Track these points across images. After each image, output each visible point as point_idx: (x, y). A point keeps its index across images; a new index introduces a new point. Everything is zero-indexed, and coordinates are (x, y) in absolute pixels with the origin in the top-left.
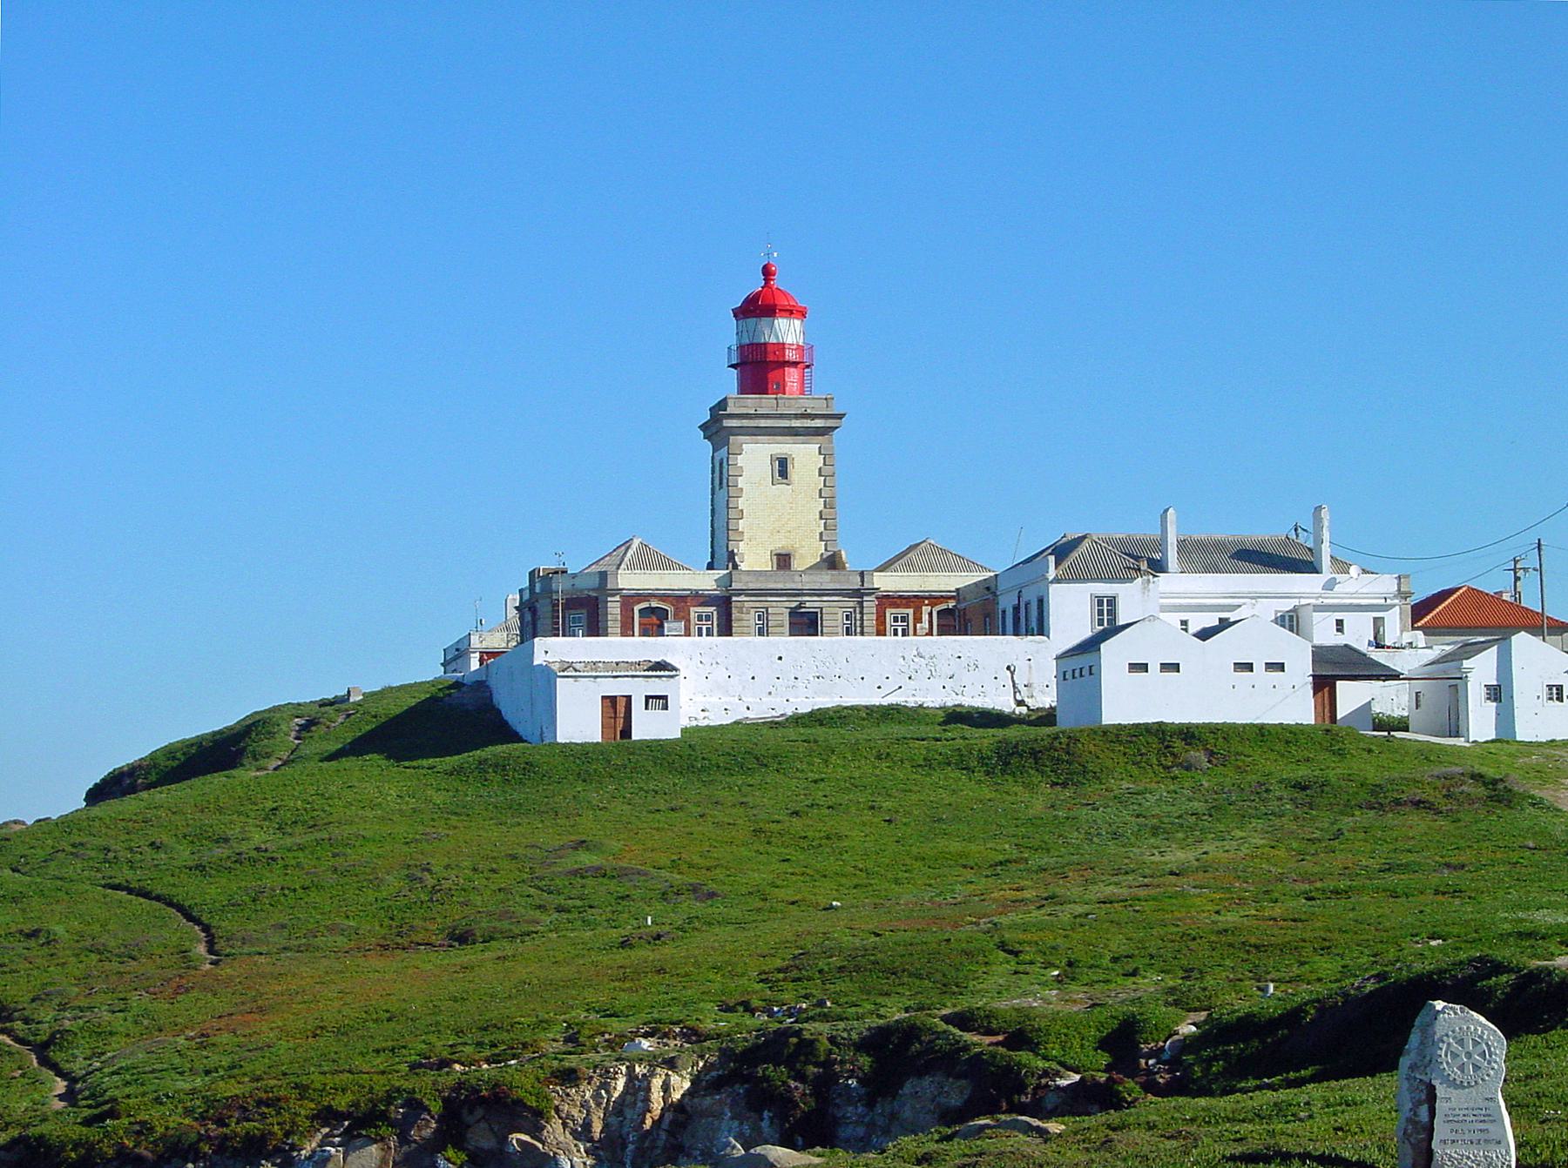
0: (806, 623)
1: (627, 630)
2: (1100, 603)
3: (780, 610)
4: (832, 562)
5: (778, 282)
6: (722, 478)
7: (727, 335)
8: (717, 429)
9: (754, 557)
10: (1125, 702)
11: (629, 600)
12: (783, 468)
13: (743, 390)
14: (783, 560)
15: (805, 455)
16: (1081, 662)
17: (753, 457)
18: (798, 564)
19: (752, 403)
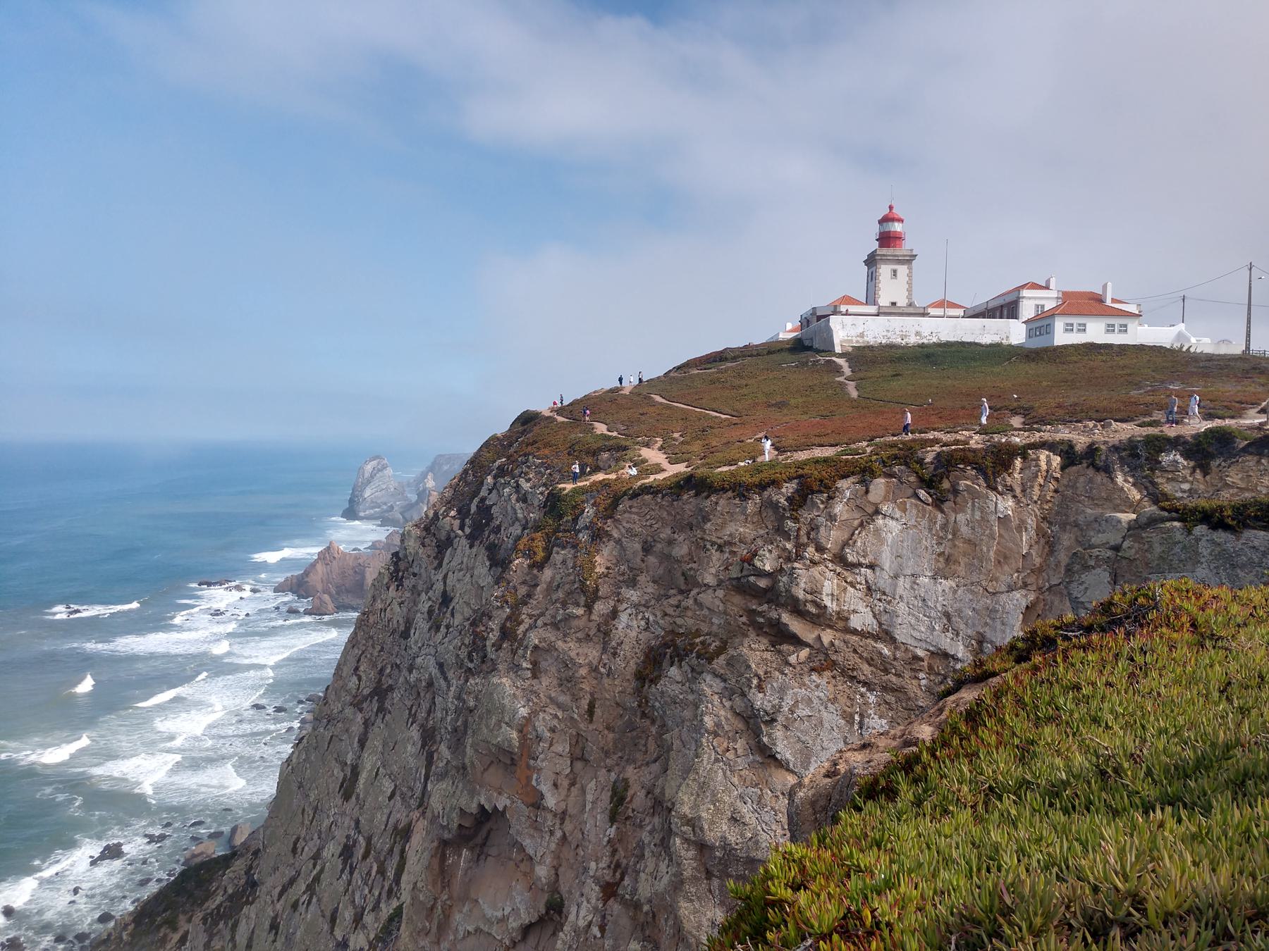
2: (1037, 306)
4: (910, 305)
6: (872, 278)
7: (875, 230)
10: (1062, 336)
13: (881, 246)
15: (902, 270)
17: (884, 270)
19: (884, 251)
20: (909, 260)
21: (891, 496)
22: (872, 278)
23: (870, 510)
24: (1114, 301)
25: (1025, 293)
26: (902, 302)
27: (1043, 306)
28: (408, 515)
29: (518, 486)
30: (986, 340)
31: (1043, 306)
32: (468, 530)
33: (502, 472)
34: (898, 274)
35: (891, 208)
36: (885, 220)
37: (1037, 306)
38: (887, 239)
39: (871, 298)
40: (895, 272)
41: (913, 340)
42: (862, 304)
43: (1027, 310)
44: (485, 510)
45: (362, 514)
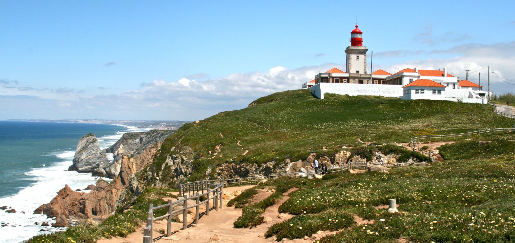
0: (361, 82)
1: (333, 82)
2: (410, 79)
3: (357, 80)
5: (358, 28)
6: (348, 59)
7: (350, 36)
8: (348, 51)
9: (353, 71)
10: (415, 96)
11: (333, 78)
12: (358, 57)
13: (352, 44)
14: (358, 72)
15: (361, 56)
16: (407, 90)
18: (360, 73)
19: (353, 47)
20: (364, 52)
21: (303, 166)
22: (348, 59)
23: (298, 170)
24: (449, 75)
25: (405, 74)
26: (361, 72)
27: (412, 79)
28: (107, 170)
29: (183, 160)
30: (386, 95)
31: (412, 79)
32: (160, 177)
33: (174, 153)
34: (360, 58)
35: (357, 27)
36: (353, 33)
37: (410, 79)
38: (356, 42)
39: (347, 71)
40: (358, 57)
41: (356, 94)
42: (342, 72)
43: (406, 81)
44: (168, 167)
45: (80, 169)
